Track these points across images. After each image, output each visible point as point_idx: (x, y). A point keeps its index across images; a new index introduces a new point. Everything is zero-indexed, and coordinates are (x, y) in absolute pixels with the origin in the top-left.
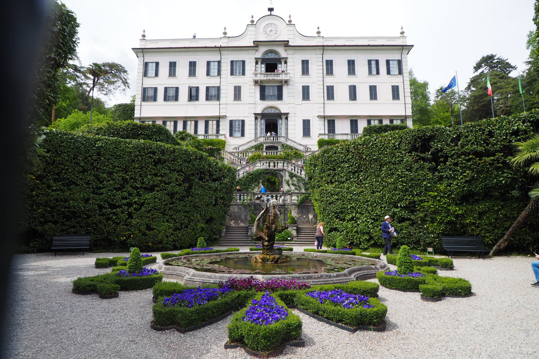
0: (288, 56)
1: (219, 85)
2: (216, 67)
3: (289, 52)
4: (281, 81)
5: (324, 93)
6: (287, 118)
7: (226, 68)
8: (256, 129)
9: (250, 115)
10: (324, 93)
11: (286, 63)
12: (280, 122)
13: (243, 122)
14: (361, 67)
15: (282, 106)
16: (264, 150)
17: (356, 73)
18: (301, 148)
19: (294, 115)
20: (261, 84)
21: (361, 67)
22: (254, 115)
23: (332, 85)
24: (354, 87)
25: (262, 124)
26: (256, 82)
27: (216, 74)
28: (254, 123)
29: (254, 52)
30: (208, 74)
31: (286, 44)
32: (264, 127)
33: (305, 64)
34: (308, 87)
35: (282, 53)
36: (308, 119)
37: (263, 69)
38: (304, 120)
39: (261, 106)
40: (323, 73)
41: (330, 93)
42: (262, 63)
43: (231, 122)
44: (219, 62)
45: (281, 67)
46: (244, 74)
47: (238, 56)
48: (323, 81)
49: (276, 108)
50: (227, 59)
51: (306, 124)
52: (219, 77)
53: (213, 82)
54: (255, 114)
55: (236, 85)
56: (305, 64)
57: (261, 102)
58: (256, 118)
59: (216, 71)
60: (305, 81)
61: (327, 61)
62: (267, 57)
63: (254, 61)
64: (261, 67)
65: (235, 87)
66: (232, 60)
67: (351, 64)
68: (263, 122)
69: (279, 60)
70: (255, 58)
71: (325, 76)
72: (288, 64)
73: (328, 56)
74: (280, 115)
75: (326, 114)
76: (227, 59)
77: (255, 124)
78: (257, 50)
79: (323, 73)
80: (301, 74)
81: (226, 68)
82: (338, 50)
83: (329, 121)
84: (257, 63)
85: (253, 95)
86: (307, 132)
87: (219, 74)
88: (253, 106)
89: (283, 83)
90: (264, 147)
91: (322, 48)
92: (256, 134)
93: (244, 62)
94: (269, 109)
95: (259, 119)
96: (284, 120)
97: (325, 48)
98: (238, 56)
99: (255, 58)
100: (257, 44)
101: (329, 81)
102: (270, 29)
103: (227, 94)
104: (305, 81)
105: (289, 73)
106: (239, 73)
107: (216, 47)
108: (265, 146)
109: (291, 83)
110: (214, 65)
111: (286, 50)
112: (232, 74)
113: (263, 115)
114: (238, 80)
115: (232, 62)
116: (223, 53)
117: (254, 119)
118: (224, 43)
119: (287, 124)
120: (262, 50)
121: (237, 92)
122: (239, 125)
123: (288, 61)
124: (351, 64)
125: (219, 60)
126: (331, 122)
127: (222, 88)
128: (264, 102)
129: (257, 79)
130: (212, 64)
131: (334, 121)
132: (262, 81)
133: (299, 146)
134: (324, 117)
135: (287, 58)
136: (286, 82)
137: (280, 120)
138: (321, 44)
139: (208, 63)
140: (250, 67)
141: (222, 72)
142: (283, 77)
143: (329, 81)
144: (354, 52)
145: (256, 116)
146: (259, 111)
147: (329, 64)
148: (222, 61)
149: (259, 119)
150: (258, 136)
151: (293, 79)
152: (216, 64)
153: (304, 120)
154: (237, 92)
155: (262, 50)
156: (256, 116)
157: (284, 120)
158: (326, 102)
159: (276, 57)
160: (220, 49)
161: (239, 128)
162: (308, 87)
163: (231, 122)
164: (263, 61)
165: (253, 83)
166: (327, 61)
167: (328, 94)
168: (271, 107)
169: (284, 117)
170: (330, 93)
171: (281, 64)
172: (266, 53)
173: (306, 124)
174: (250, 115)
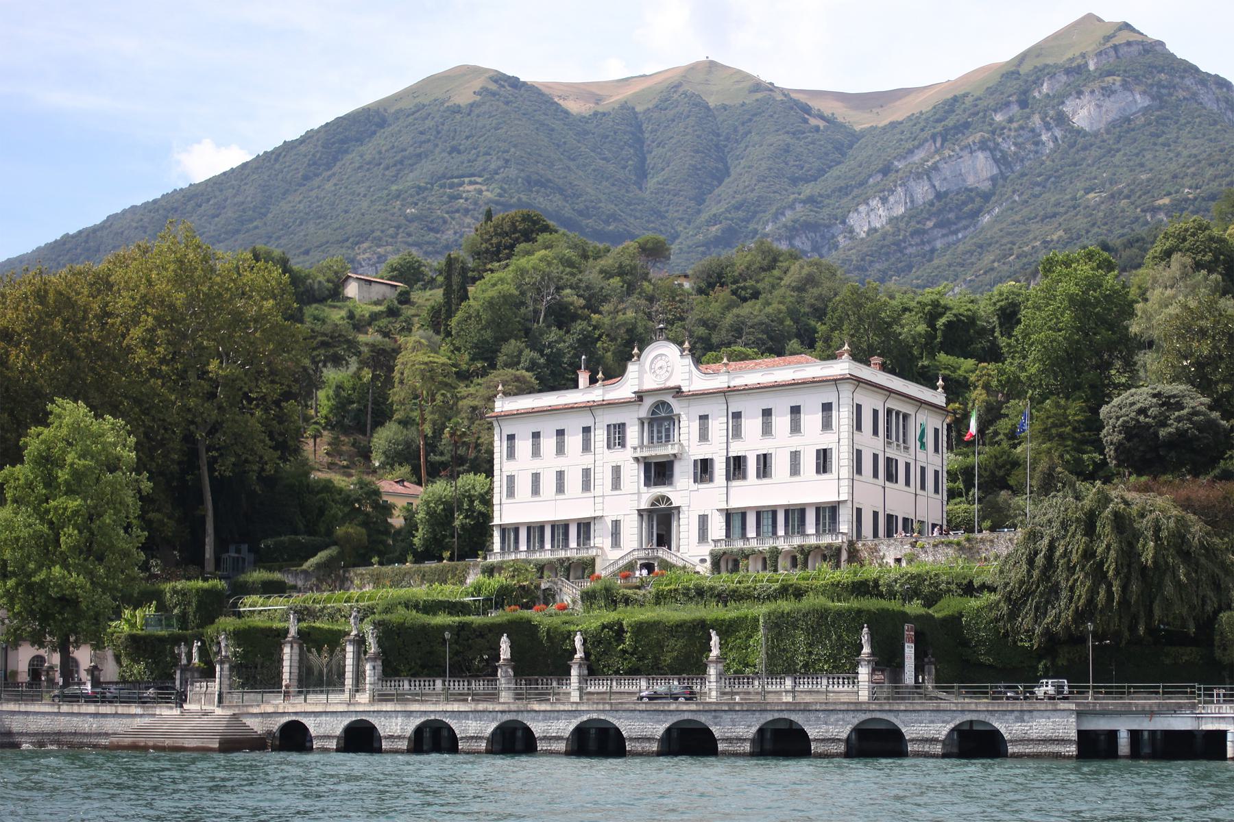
26: (637, 459)
31: (678, 392)
47: (615, 417)
53: (587, 461)
70: (639, 419)
86: (703, 536)
98: (615, 417)
99: (639, 419)
100: (640, 397)
102: (659, 365)
108: (639, 562)
112: (609, 447)
129: (636, 455)
132: (645, 458)
140: (633, 434)
143: (736, 449)
145: (640, 513)
155: (649, 402)
156: (640, 513)
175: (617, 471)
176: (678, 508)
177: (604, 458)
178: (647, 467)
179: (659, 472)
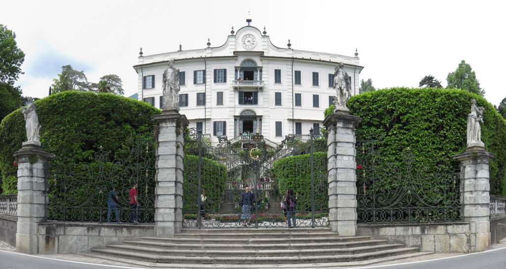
0: (264, 66)
1: (204, 92)
2: (202, 76)
3: (264, 62)
4: (257, 88)
5: (293, 99)
6: (261, 120)
7: (210, 77)
8: (235, 129)
9: (230, 117)
10: (293, 99)
11: (261, 71)
12: (255, 122)
13: (225, 123)
14: (324, 80)
15: (258, 110)
16: (242, 147)
17: (319, 85)
18: (275, 146)
19: (268, 117)
20: (240, 90)
21: (324, 80)
22: (233, 117)
23: (300, 93)
24: (317, 96)
25: (240, 123)
26: (236, 89)
27: (202, 82)
28: (233, 124)
29: (234, 61)
30: (195, 83)
32: (242, 127)
33: (278, 73)
34: (280, 94)
35: (259, 64)
36: (280, 121)
37: (243, 76)
38: (276, 122)
39: (239, 110)
40: (292, 82)
41: (298, 100)
42: (240, 71)
43: (215, 123)
44: (204, 72)
45: (257, 75)
46: (225, 81)
47: (220, 66)
48: (292, 89)
49: (253, 112)
50: (211, 69)
51: (279, 125)
52: (204, 84)
54: (235, 116)
55: (219, 91)
56: (278, 73)
57: (240, 106)
58: (235, 120)
59: (202, 79)
60: (278, 88)
61: (296, 72)
62: (246, 66)
63: (234, 69)
64: (240, 75)
65: (218, 93)
66: (215, 69)
67: (315, 77)
68: (241, 122)
69: (256, 69)
70: (235, 67)
71: (294, 85)
72: (263, 73)
73: (297, 68)
74: (255, 117)
75: (296, 117)
76: (211, 69)
77: (235, 124)
78: (236, 60)
79: (292, 82)
80: (274, 82)
81: (210, 77)
82: (305, 63)
83: (297, 124)
84: (236, 71)
85: (233, 100)
86: (279, 132)
87: (204, 82)
88: (233, 109)
89: (259, 89)
90: (242, 145)
91: (292, 60)
92: (235, 133)
93: (225, 70)
94: (246, 112)
95: (238, 121)
96: (258, 122)
97: (294, 60)
101: (298, 89)
103: (211, 99)
104: (278, 88)
105: (263, 81)
106: (222, 81)
107: (201, 58)
109: (264, 90)
110: (200, 74)
111: (261, 60)
112: (215, 81)
113: (241, 117)
114: (220, 87)
115: (215, 71)
116: (207, 62)
117: (233, 120)
118: (208, 54)
119: (261, 125)
120: (241, 59)
121: (220, 97)
122: (221, 126)
123: (263, 70)
124: (315, 77)
125: (204, 69)
126: (298, 124)
127: (207, 94)
128: (242, 106)
129: (237, 86)
130: (198, 73)
131: (300, 124)
132: (240, 88)
133: (273, 144)
134: (293, 120)
135: (262, 67)
136: (261, 89)
137: (255, 122)
138: (291, 56)
139: (195, 73)
140: (231, 76)
141: (207, 80)
142: (258, 85)
143: (298, 89)
144: (318, 66)
145: (236, 118)
146: (238, 114)
147: (298, 75)
148: (207, 70)
149: (238, 121)
150: (237, 136)
151: (267, 86)
152: (202, 72)
153: (276, 122)
154: (220, 97)
155: (241, 59)
156: (236, 118)
157: (258, 122)
158: (295, 107)
159: (253, 65)
160: (205, 60)
161: (221, 128)
162: (280, 93)
163: (215, 123)
164: (242, 69)
165: (232, 89)
166: (296, 72)
167: (296, 100)
168: (248, 110)
169: (258, 119)
170: (298, 100)
171: (257, 71)
172: (244, 62)
173: (279, 125)
174: (230, 117)
175: (220, 96)
176: (260, 118)
177: (212, 89)
178: (241, 94)
179: (248, 97)
